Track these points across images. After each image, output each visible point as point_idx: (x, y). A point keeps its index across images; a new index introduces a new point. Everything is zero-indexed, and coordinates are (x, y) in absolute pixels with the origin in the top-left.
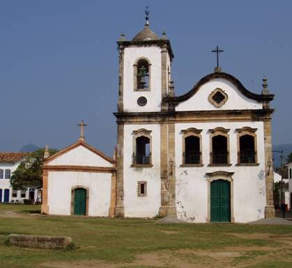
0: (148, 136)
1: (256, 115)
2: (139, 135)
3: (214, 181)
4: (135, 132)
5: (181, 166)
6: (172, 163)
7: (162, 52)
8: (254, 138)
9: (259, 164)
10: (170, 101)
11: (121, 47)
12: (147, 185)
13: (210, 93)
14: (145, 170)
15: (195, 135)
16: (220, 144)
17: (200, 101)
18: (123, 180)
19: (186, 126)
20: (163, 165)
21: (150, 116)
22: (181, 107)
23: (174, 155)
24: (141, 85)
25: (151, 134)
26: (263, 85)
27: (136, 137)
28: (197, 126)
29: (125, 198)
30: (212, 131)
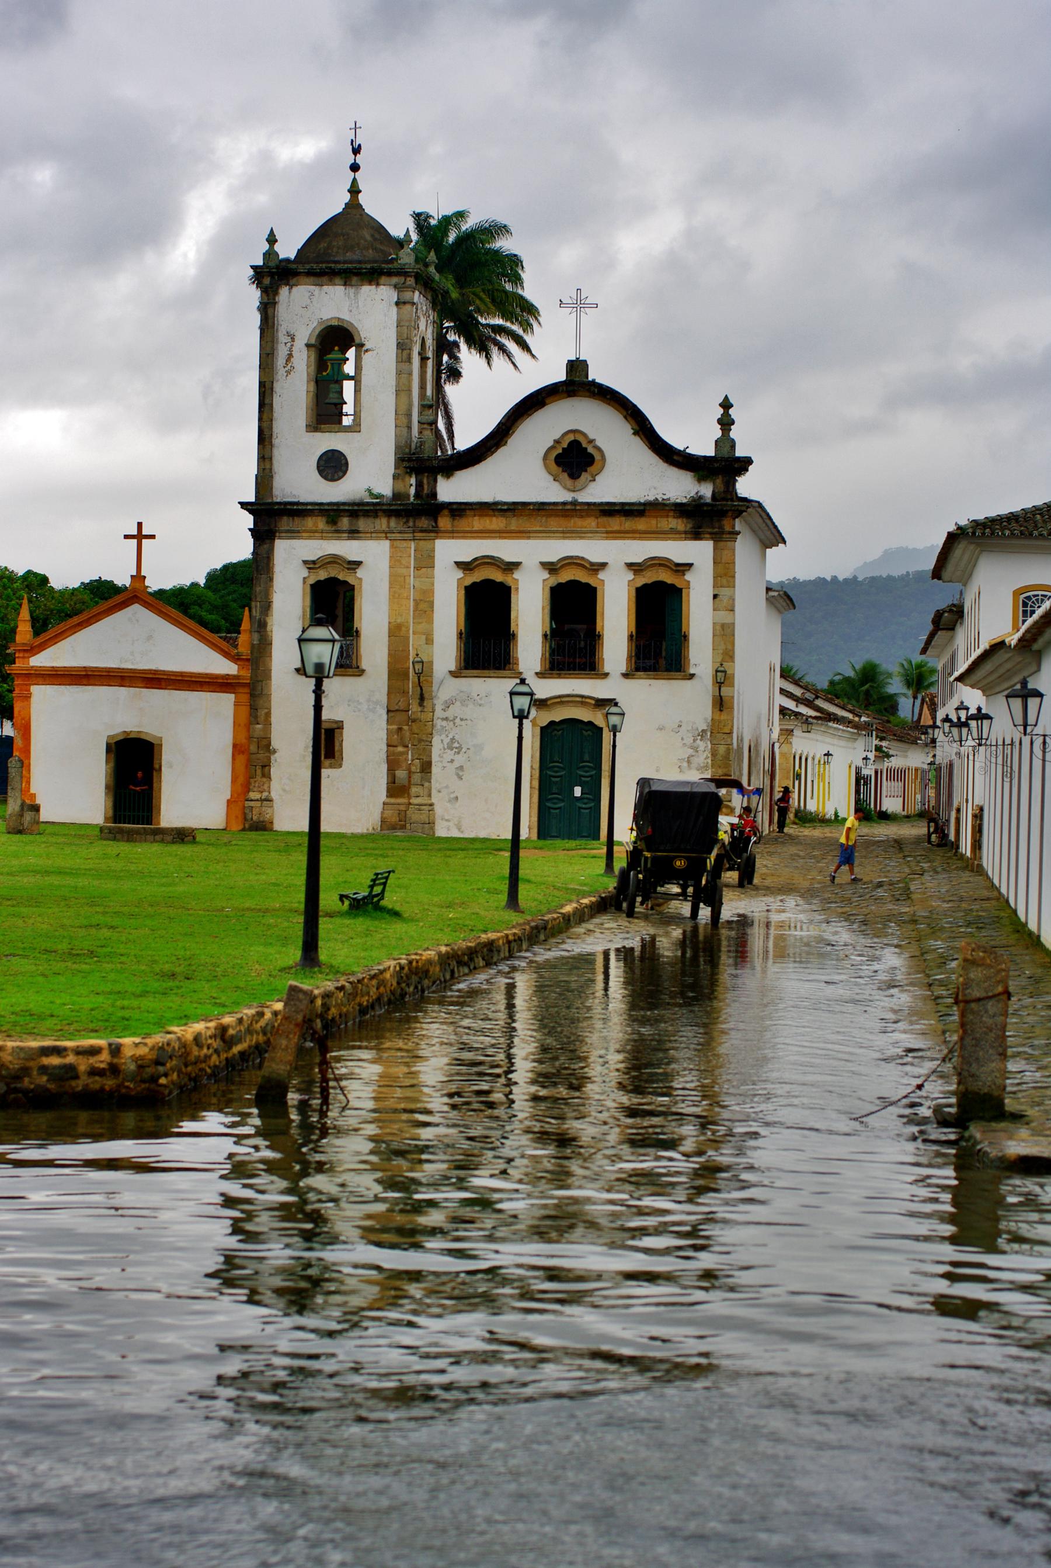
0: (351, 580)
2: (323, 575)
3: (552, 723)
4: (311, 565)
5: (454, 674)
6: (424, 671)
7: (397, 304)
8: (681, 590)
9: (692, 676)
11: (267, 281)
12: (345, 731)
13: (551, 443)
15: (498, 576)
18: (268, 715)
19: (469, 549)
20: (397, 673)
23: (429, 641)
25: (360, 573)
26: (719, 421)
27: (312, 581)
28: (505, 549)
29: (274, 771)
30: (551, 567)
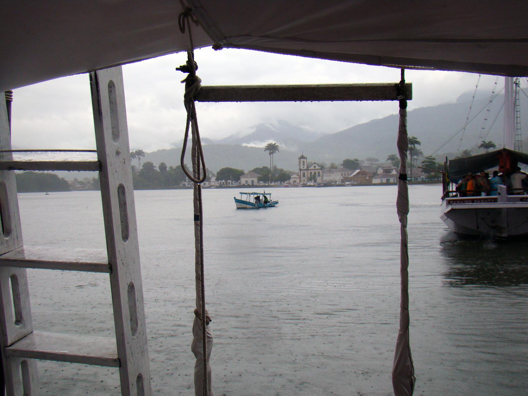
1: (321, 169)
4: (303, 172)
10: (308, 167)
14: (305, 178)
16: (315, 173)
17: (312, 168)
20: (307, 177)
21: (305, 170)
22: (309, 168)
24: (304, 165)
